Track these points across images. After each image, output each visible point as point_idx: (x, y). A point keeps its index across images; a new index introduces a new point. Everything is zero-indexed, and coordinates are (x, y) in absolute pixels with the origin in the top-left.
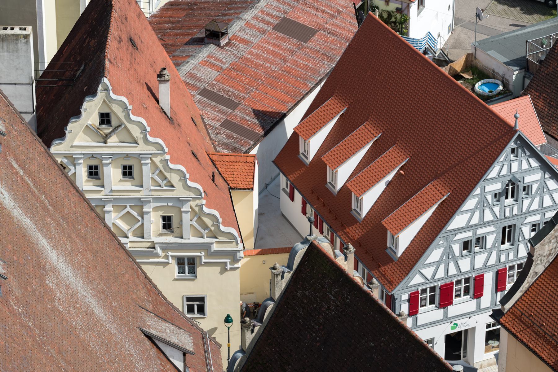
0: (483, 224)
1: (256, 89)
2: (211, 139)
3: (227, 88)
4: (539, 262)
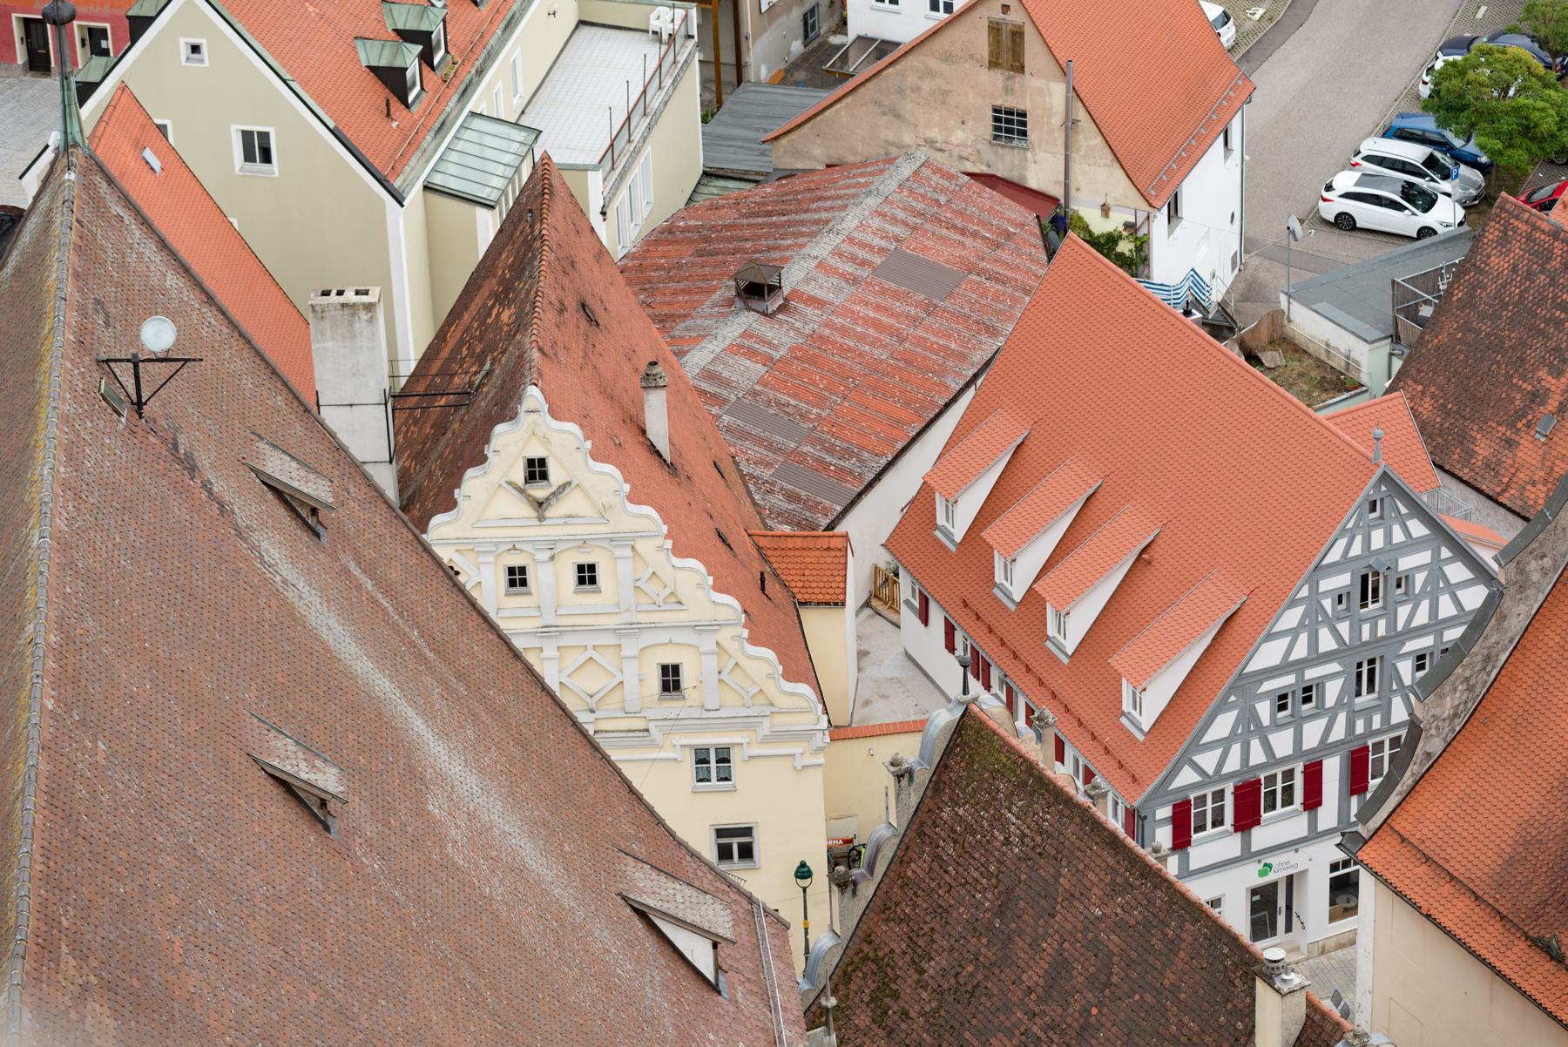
0: (1317, 658)
1: (845, 398)
2: (754, 504)
3: (784, 398)
4: (1433, 732)
